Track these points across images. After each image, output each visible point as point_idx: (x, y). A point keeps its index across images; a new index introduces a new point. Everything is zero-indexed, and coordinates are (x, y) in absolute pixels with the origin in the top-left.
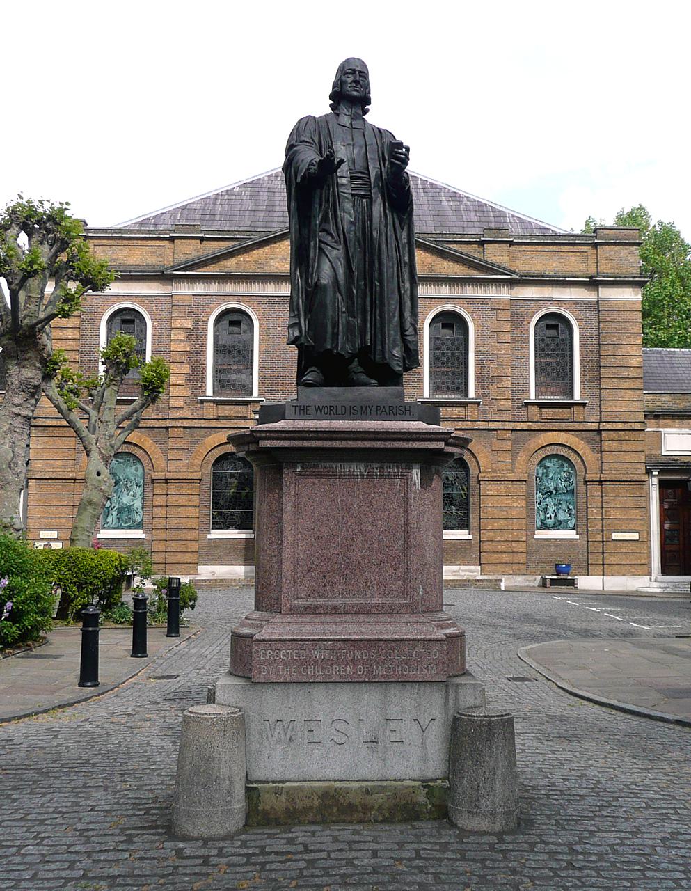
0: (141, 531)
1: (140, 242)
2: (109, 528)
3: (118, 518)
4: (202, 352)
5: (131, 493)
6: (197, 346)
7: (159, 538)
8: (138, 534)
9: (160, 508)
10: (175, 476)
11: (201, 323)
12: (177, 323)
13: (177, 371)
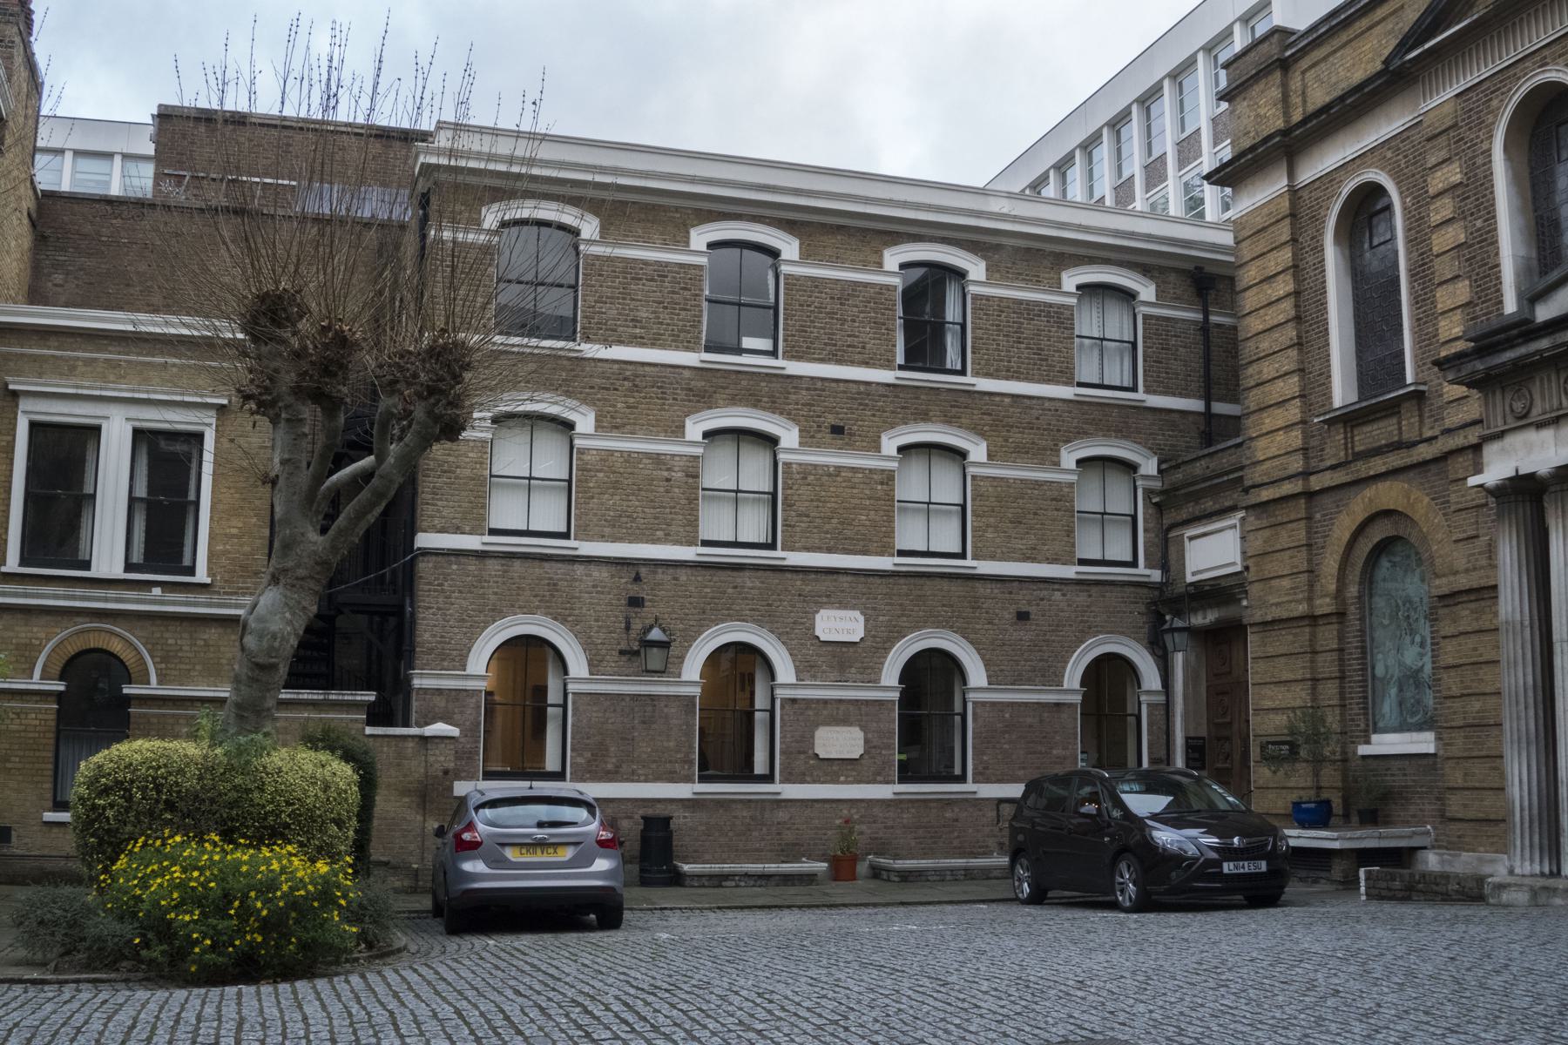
0: (1429, 736)
1: (1364, 23)
2: (1386, 731)
3: (1400, 704)
4: (1487, 238)
5: (1418, 639)
6: (1479, 223)
7: (1455, 751)
8: (1423, 743)
9: (1453, 673)
10: (1463, 582)
11: (1480, 161)
12: (1437, 182)
13: (1450, 304)
